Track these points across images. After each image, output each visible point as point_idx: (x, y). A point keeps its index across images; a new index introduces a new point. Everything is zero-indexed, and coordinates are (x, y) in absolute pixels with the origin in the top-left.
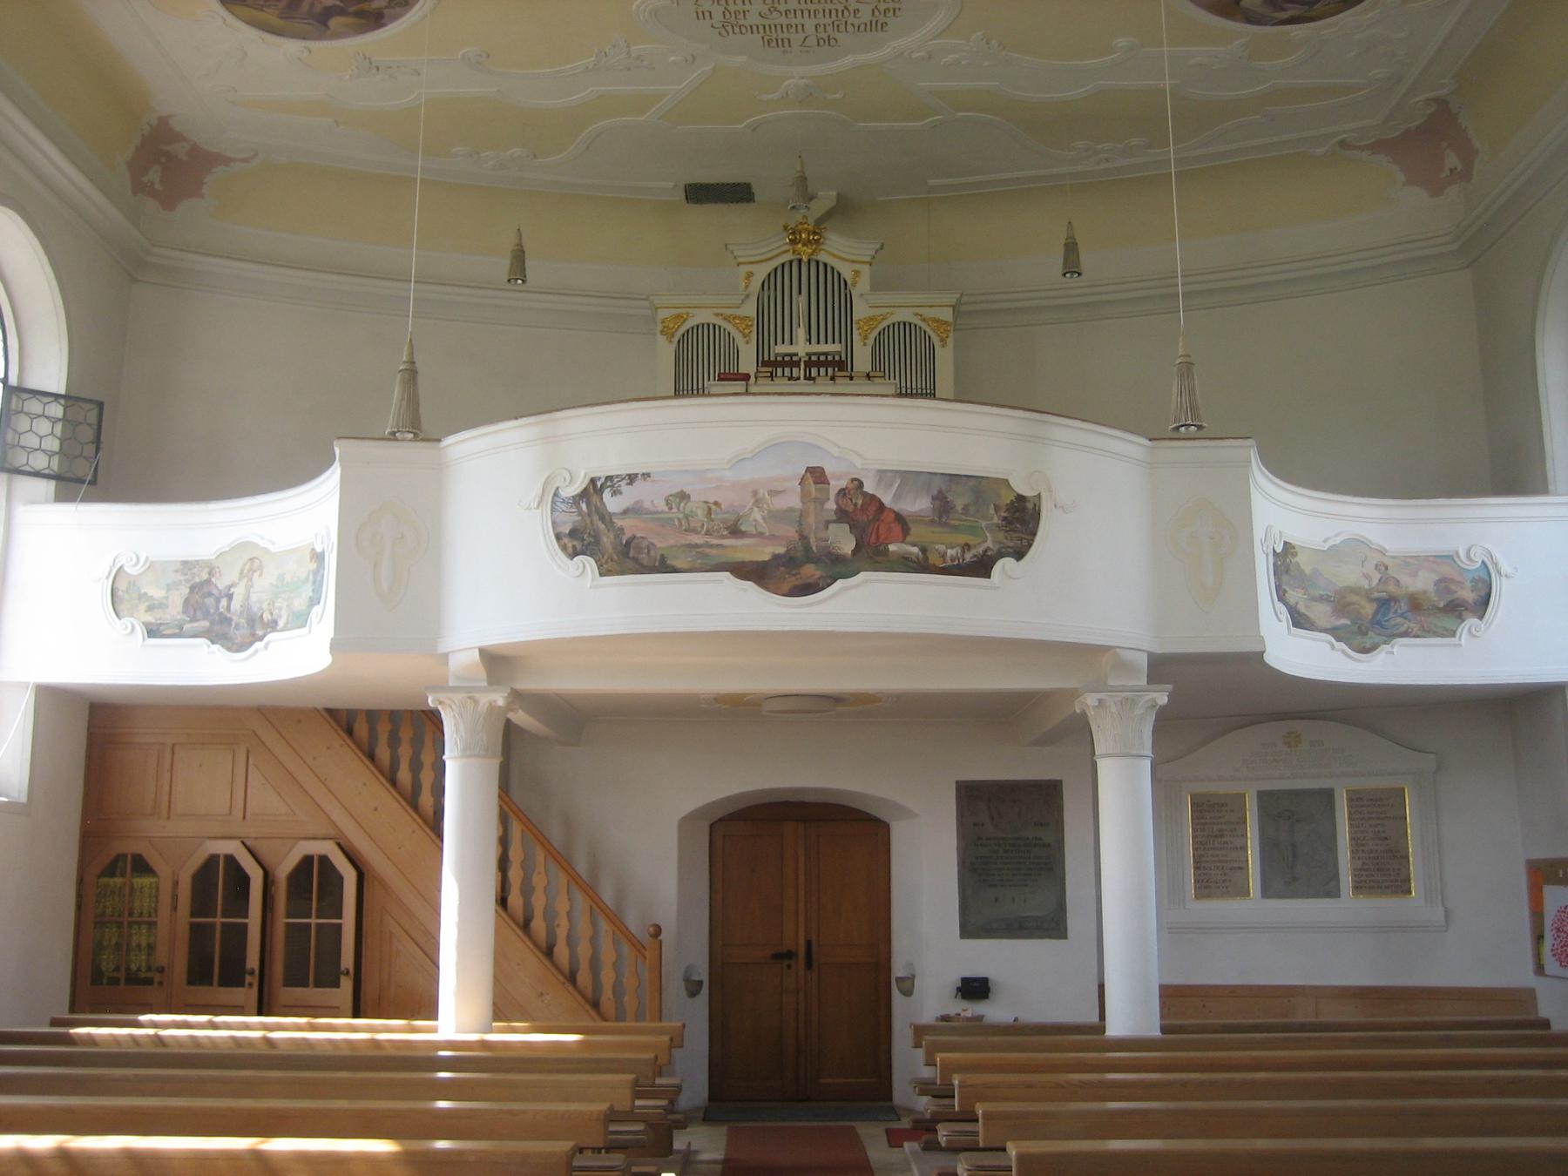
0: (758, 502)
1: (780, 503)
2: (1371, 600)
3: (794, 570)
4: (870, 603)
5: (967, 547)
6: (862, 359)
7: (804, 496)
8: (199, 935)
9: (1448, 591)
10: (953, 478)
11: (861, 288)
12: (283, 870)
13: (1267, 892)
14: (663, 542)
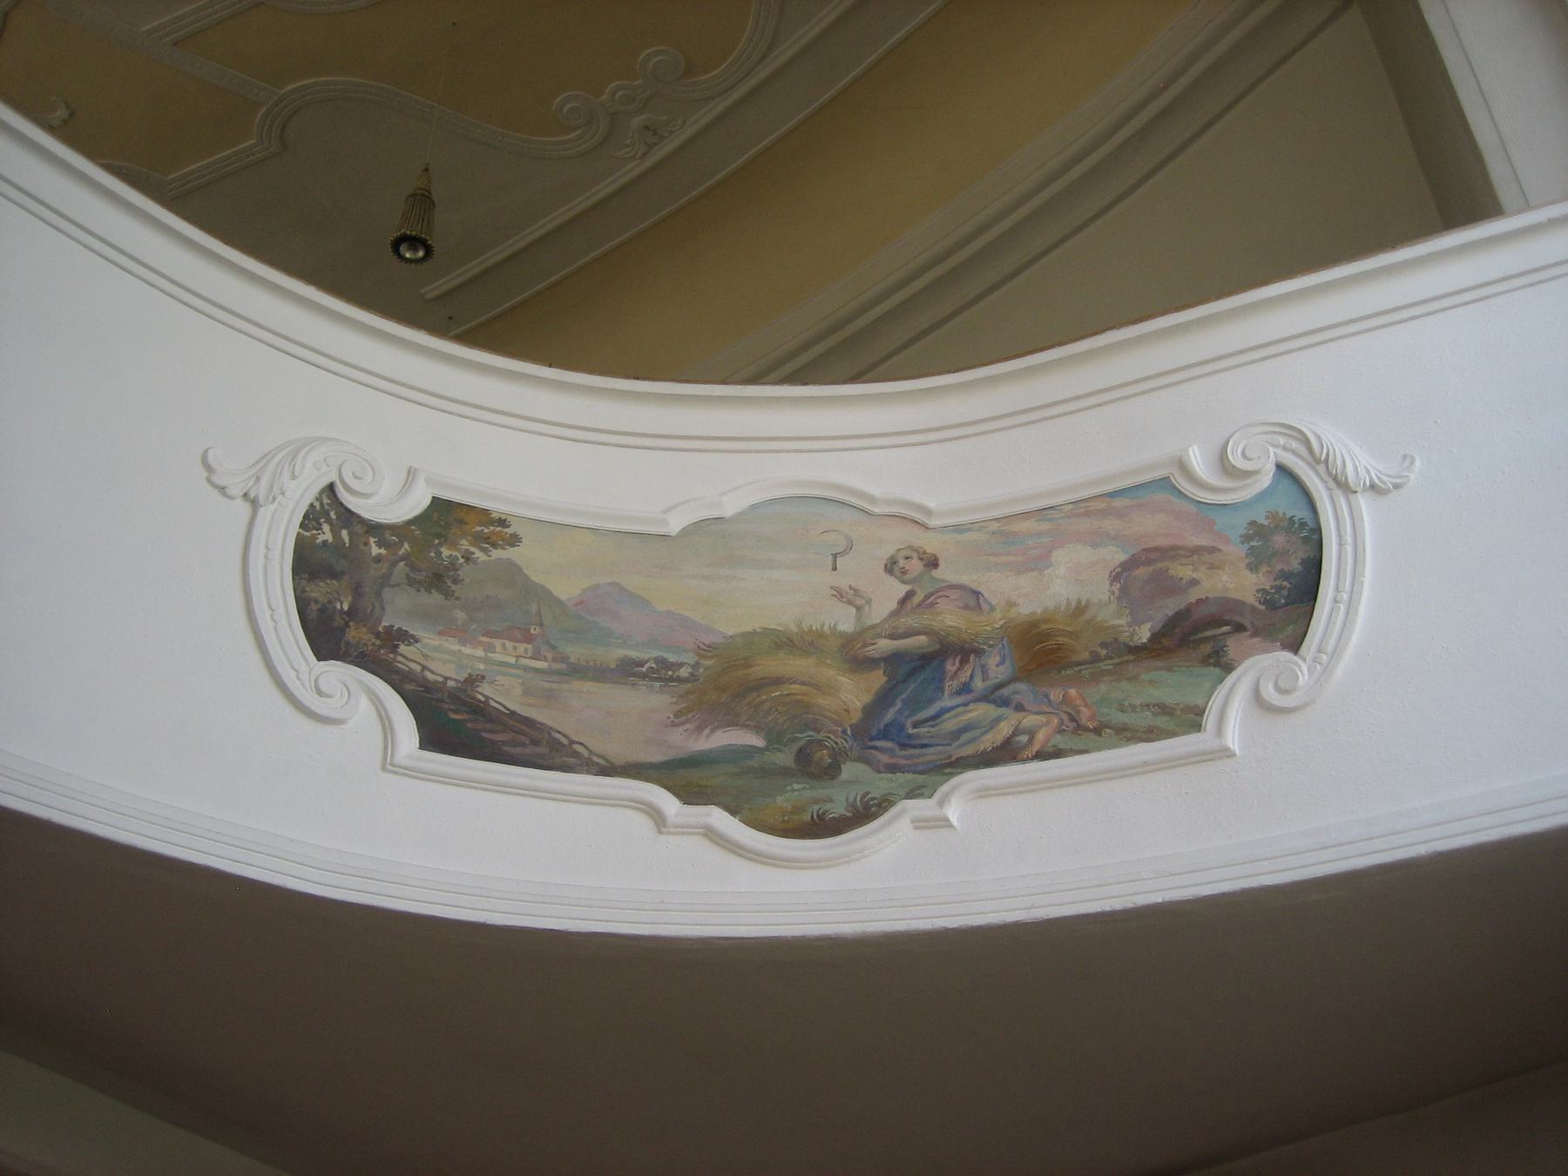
2: (860, 663)
9: (1165, 586)
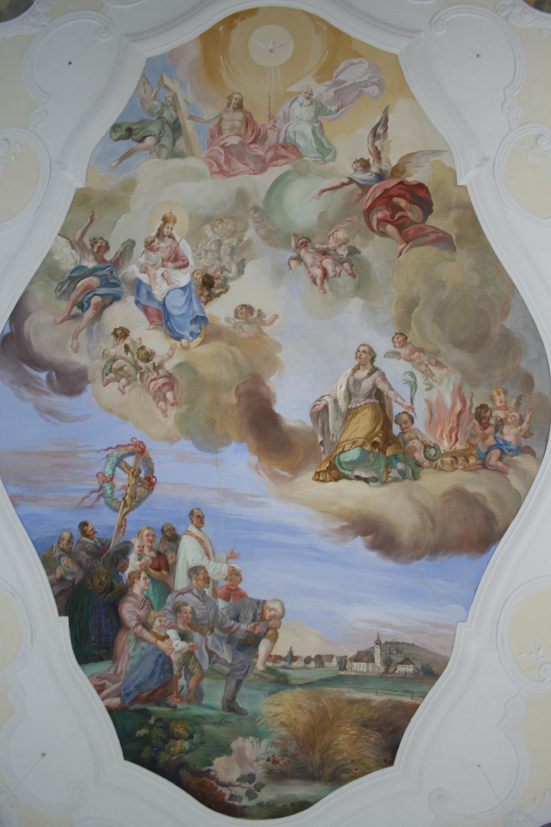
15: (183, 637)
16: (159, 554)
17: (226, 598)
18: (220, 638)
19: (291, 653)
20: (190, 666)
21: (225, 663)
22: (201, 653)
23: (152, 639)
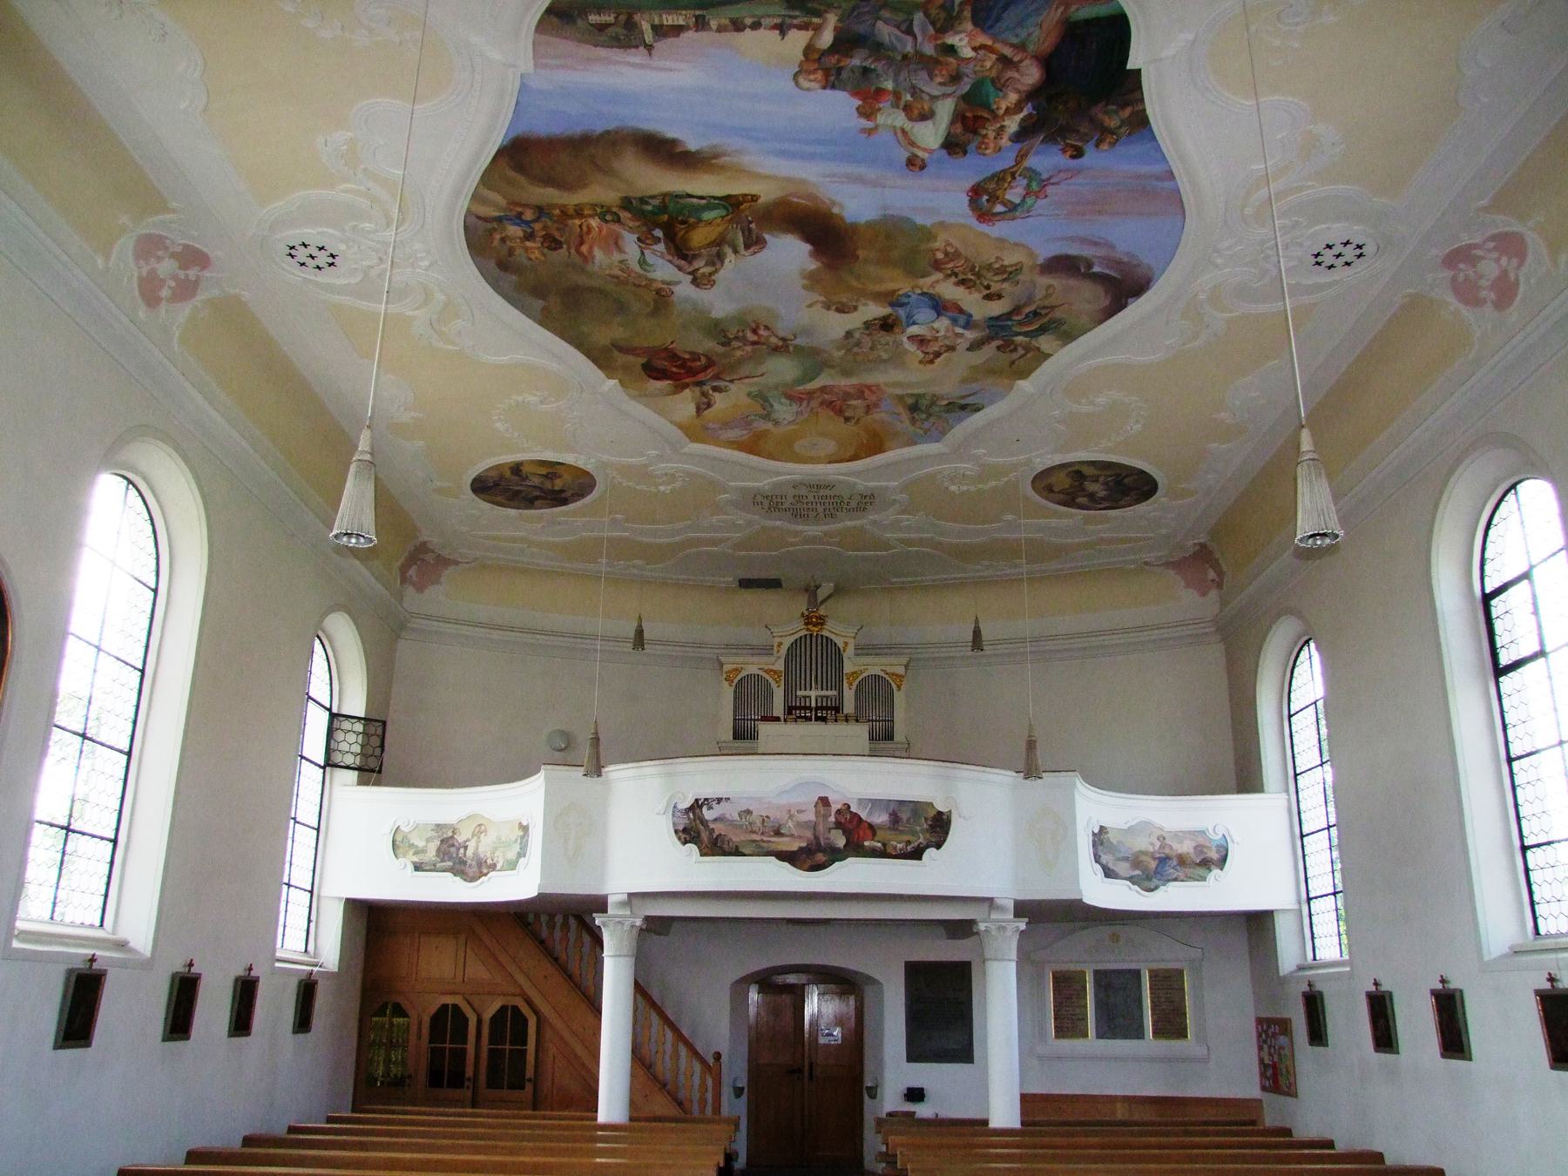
0: (791, 817)
1: (803, 818)
3: (811, 857)
4: (851, 874)
5: (909, 842)
6: (849, 707)
7: (817, 813)
8: (436, 1054)
9: (1202, 852)
10: (901, 803)
11: (849, 653)
12: (487, 1015)
13: (1100, 1036)
14: (737, 838)
15: (951, 50)
16: (975, 132)
17: (880, 92)
18: (894, 49)
19: (783, 33)
20: (943, 15)
21: (886, 22)
22: (924, 31)
23: (998, 46)
